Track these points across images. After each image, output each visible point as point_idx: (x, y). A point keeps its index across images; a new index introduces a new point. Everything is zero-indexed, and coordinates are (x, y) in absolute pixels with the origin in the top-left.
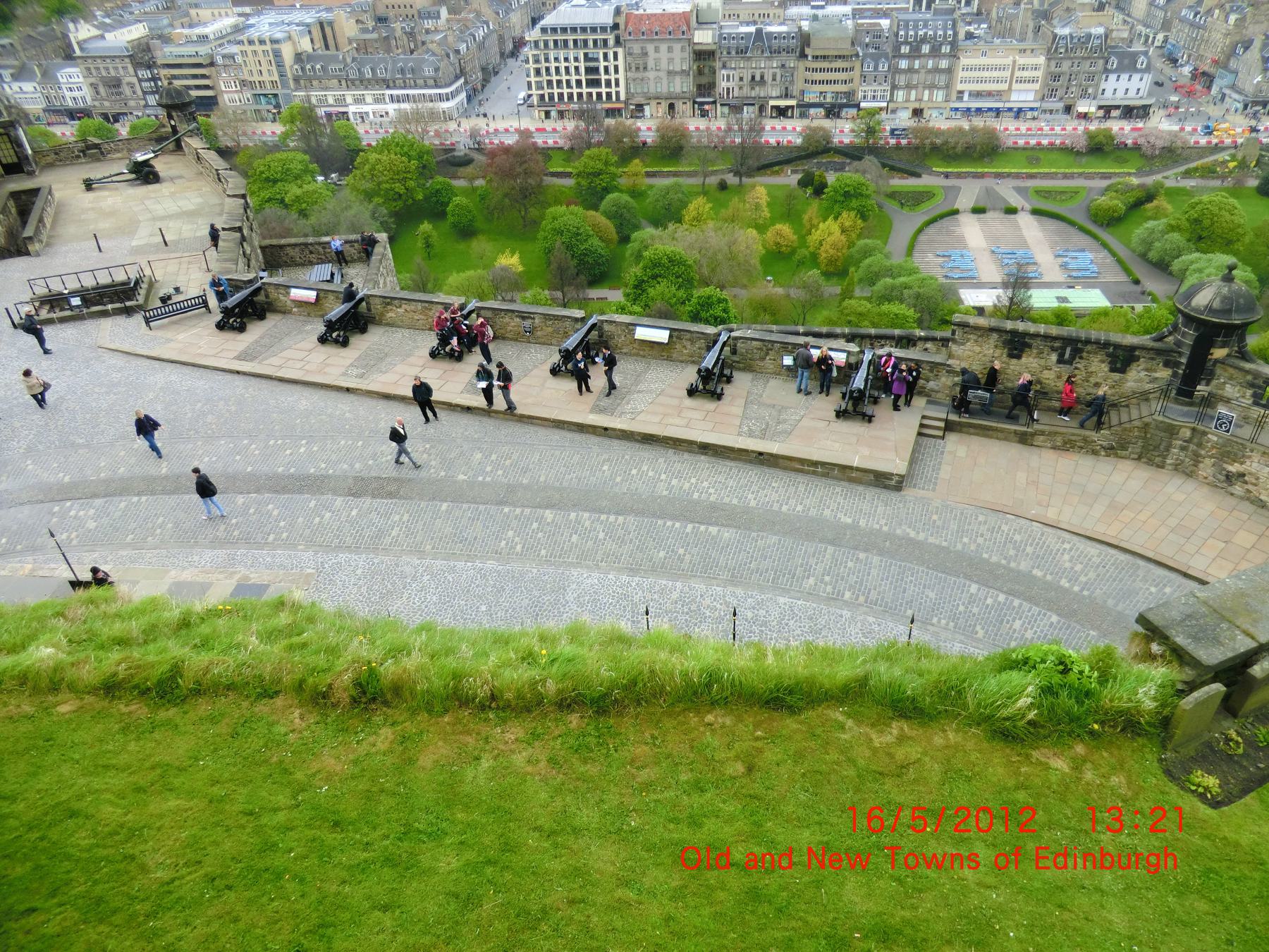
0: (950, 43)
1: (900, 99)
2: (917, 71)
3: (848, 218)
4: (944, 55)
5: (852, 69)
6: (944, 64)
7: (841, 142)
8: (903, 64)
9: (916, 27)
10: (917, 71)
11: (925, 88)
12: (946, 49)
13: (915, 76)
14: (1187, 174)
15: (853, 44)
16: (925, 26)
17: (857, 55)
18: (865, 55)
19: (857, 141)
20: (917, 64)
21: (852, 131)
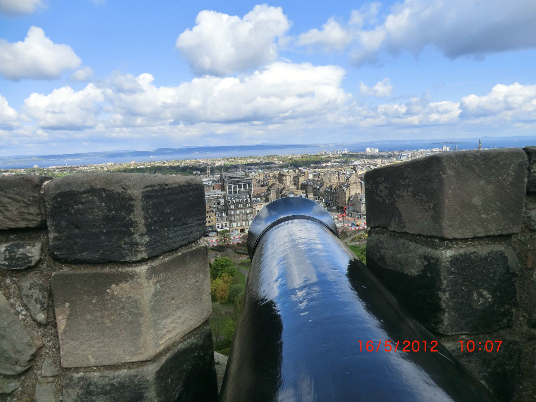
0: (250, 203)
1: (234, 226)
2: (239, 215)
3: (225, 276)
4: (249, 208)
5: (212, 216)
6: (249, 211)
7: (213, 246)
8: (232, 212)
9: (235, 198)
10: (239, 215)
11: (243, 221)
12: (248, 205)
13: (238, 217)
14: (353, 240)
15: (210, 207)
16: (238, 198)
17: (212, 211)
18: (216, 211)
19: (220, 244)
20: (238, 212)
21: (217, 240)
